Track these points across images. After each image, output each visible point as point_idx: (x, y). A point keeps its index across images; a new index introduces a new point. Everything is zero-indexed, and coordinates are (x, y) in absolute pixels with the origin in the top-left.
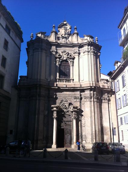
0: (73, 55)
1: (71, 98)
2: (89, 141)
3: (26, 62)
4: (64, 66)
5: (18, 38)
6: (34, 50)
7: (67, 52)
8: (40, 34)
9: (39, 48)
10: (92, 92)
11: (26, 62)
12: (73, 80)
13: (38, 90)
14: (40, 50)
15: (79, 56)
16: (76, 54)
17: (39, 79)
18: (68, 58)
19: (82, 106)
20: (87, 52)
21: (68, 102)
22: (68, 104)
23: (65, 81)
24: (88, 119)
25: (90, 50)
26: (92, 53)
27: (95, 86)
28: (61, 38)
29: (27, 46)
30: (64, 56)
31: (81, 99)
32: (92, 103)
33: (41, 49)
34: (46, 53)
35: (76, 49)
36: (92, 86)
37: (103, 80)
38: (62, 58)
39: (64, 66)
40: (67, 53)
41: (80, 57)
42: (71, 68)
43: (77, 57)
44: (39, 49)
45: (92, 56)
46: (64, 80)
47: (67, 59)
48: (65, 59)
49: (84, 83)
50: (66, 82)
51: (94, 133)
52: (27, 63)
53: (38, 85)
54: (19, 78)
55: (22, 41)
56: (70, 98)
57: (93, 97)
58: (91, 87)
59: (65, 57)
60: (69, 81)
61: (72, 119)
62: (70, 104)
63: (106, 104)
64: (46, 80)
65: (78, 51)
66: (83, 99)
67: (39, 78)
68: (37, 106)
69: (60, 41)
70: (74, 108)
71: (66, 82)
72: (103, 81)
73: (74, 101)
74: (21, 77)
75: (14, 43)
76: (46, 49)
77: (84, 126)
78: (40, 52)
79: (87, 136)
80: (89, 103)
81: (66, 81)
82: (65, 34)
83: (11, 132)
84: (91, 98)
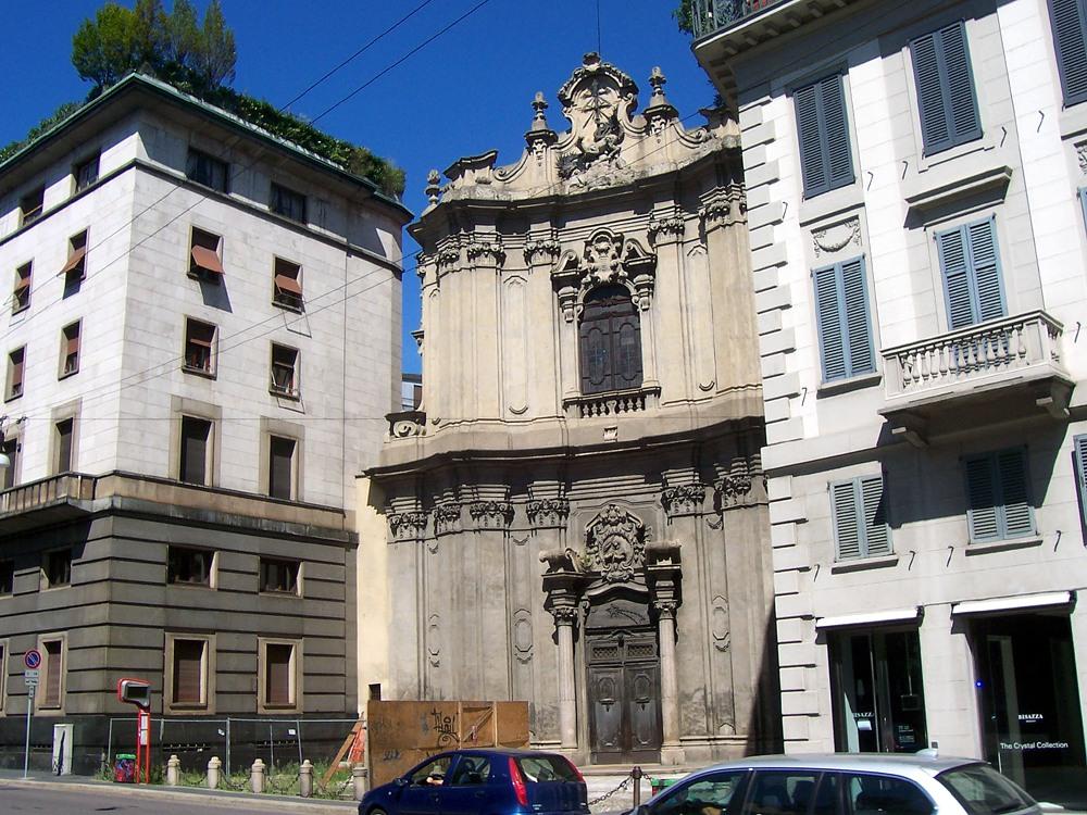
12: (657, 392)
22: (631, 536)
23: (612, 404)
42: (644, 320)
46: (606, 400)
47: (615, 277)
48: (604, 276)
50: (617, 410)
60: (638, 398)
81: (622, 405)
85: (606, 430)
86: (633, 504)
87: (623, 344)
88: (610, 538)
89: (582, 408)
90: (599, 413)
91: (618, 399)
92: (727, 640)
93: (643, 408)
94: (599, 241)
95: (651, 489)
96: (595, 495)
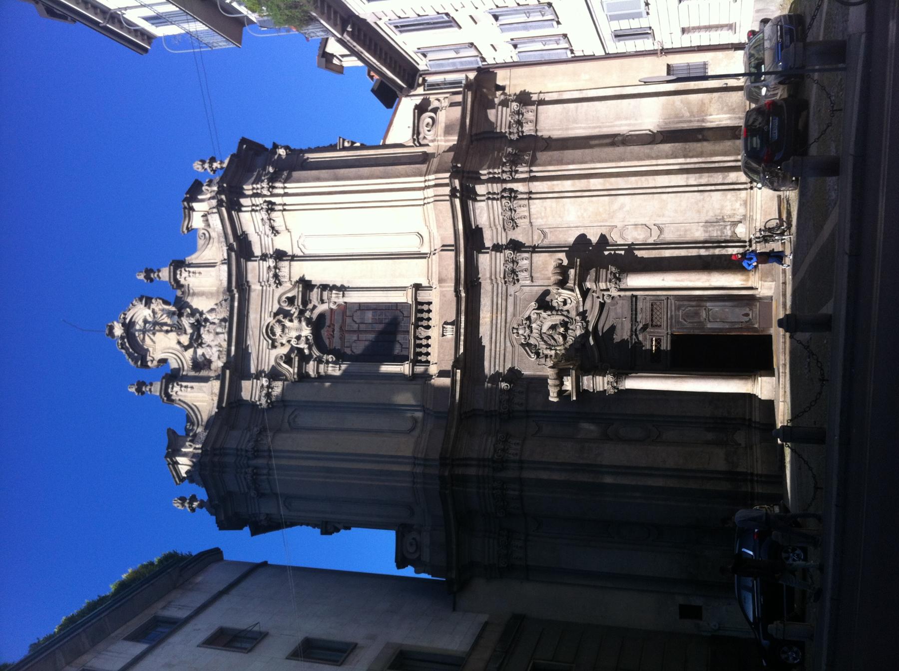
0: (287, 289)
1: (511, 300)
2: (737, 205)
3: (322, 533)
4: (347, 336)
5: (200, 579)
6: (261, 495)
7: (270, 320)
8: (180, 460)
9: (249, 467)
10: (481, 189)
11: (322, 533)
12: (417, 287)
13: (472, 471)
14: (261, 462)
15: (293, 258)
16: (284, 271)
17: (414, 464)
18: (302, 313)
19: (551, 239)
20: (274, 215)
21: (534, 317)
22: (544, 314)
23: (422, 332)
24: (622, 207)
25: (259, 201)
26: (276, 191)
27: (448, 175)
28: (200, 351)
29: (241, 528)
30: (294, 334)
31: (516, 246)
32: (537, 186)
33: (256, 457)
34: (278, 430)
35: (256, 271)
36: (447, 190)
37: (416, 131)
38: (303, 345)
39: (347, 336)
40: (279, 321)
41: (297, 252)
42: (354, 298)
43: (300, 269)
44: (256, 468)
45: (292, 187)
46: (416, 338)
47: (309, 322)
48: (306, 331)
49: (434, 231)
50: (428, 327)
51: (693, 179)
52: (328, 528)
53: (446, 474)
54: (409, 572)
55: (214, 555)
56: (515, 304)
57: (505, 181)
58: (453, 195)
59: (301, 330)
60: (422, 309)
61: (622, 293)
62: (544, 303)
63: (541, 118)
64: (416, 433)
65: (265, 265)
66: (519, 235)
67: (408, 468)
68: (556, 476)
69: (214, 358)
70: (562, 283)
71: (431, 323)
72: (424, 130)
73: (528, 282)
74: (401, 563)
75: (225, 598)
76: (255, 430)
77: (661, 230)
78: (274, 462)
79: (711, 214)
80: (536, 205)
81: (425, 323)
82: (180, 329)
83: (689, 612)
84: (512, 195)
85: (443, 335)
86: (514, 315)
87: (370, 321)
88: (545, 338)
89: (420, 361)
90: (428, 346)
91: (417, 327)
92: (653, 227)
93: (430, 303)
94: (274, 334)
95: (504, 298)
96: (502, 352)
